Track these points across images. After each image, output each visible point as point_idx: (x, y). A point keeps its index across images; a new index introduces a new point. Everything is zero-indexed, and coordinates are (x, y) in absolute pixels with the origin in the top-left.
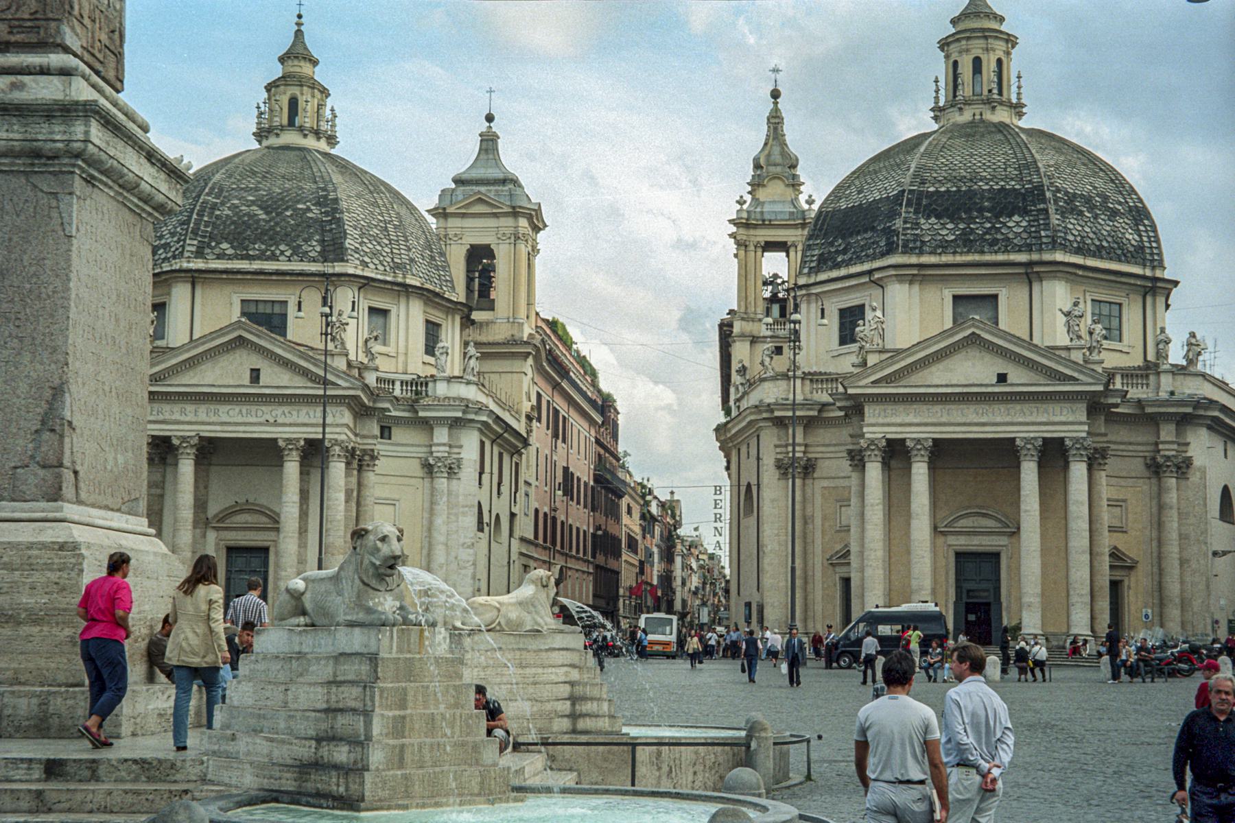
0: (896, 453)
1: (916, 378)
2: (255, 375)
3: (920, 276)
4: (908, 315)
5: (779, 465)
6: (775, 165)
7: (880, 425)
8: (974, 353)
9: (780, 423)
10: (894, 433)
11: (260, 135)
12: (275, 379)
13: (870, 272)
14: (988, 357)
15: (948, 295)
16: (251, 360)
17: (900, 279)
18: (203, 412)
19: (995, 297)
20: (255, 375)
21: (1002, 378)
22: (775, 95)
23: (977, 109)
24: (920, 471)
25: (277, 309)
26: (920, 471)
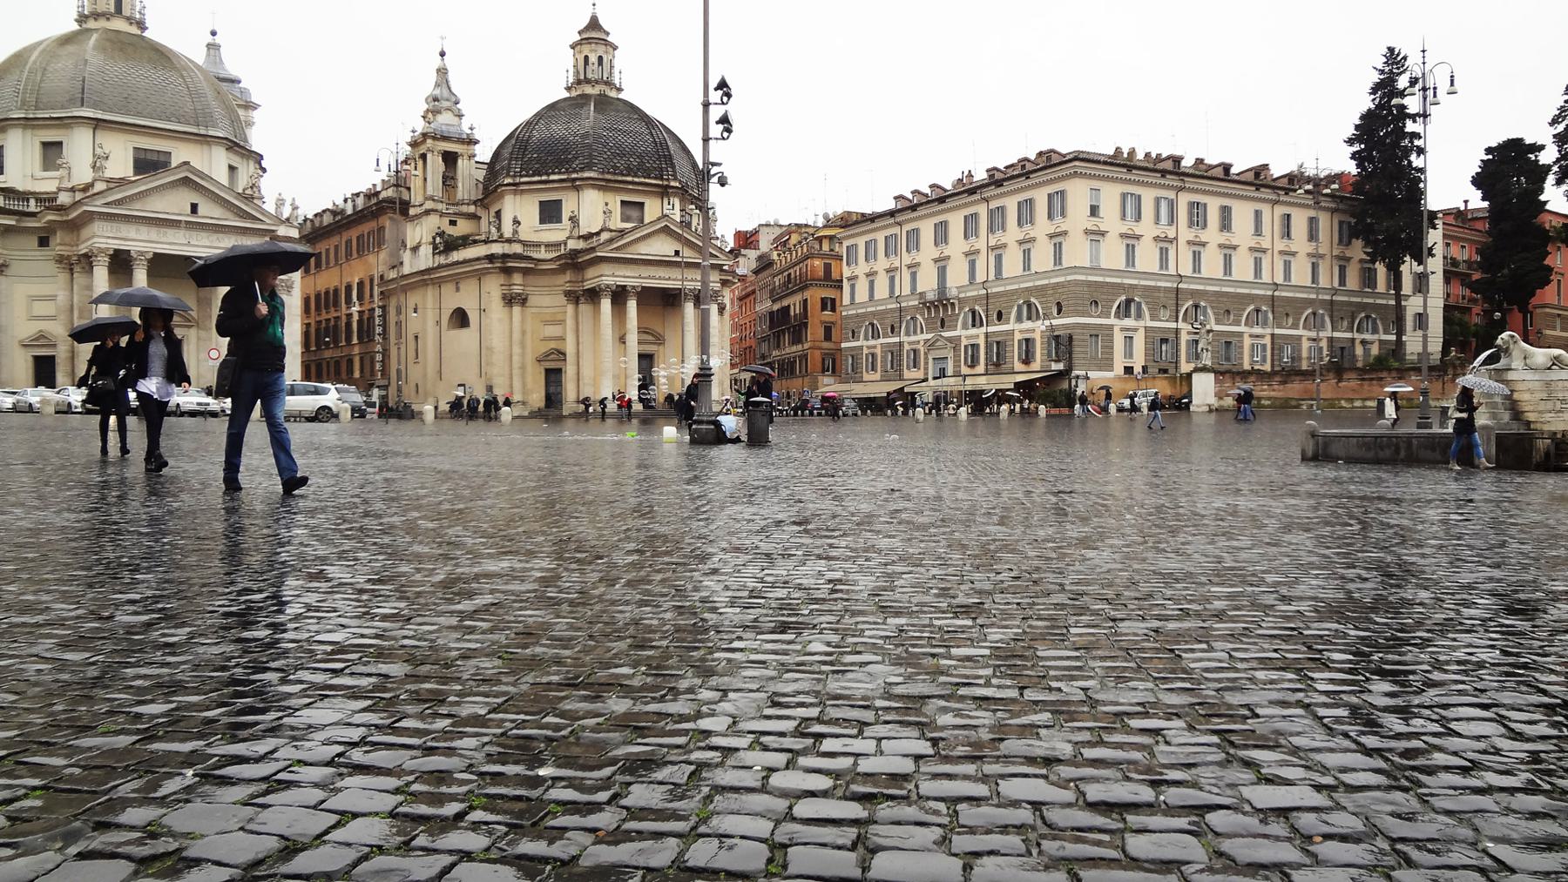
0: (619, 296)
1: (631, 249)
2: (194, 208)
3: (604, 186)
4: (593, 209)
5: (504, 297)
6: (442, 100)
7: (610, 276)
8: (663, 237)
9: (507, 271)
10: (621, 281)
11: (82, 18)
12: (209, 211)
13: (575, 180)
14: (669, 239)
15: (619, 199)
16: (190, 197)
17: (594, 187)
18: (153, 233)
19: (642, 204)
20: (194, 208)
21: (677, 253)
22: (442, 54)
23: (603, 87)
24: (632, 305)
25: (162, 158)
26: (632, 305)
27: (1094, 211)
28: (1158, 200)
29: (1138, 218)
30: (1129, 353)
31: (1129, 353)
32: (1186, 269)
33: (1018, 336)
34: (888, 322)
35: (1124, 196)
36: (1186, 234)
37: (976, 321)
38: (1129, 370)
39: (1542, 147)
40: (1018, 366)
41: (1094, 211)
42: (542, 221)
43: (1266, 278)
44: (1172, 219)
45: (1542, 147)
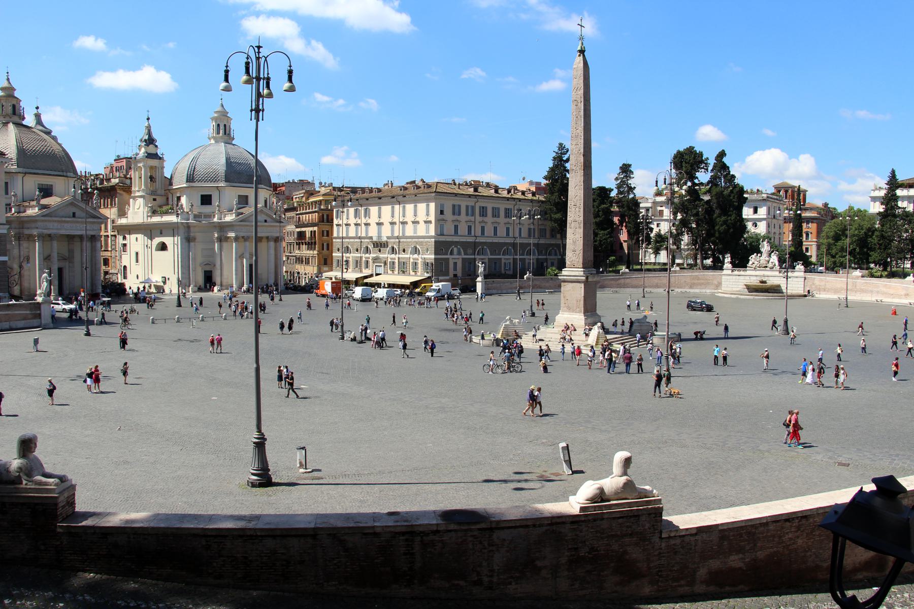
2: (74, 214)
27: (442, 212)
28: (467, 207)
29: (459, 214)
30: (455, 269)
31: (455, 269)
32: (479, 233)
33: (412, 260)
34: (355, 247)
35: (454, 206)
36: (478, 218)
37: (393, 251)
38: (455, 276)
39: (611, 190)
40: (412, 273)
41: (442, 212)
42: (202, 204)
43: (511, 235)
44: (473, 214)
45: (611, 190)
